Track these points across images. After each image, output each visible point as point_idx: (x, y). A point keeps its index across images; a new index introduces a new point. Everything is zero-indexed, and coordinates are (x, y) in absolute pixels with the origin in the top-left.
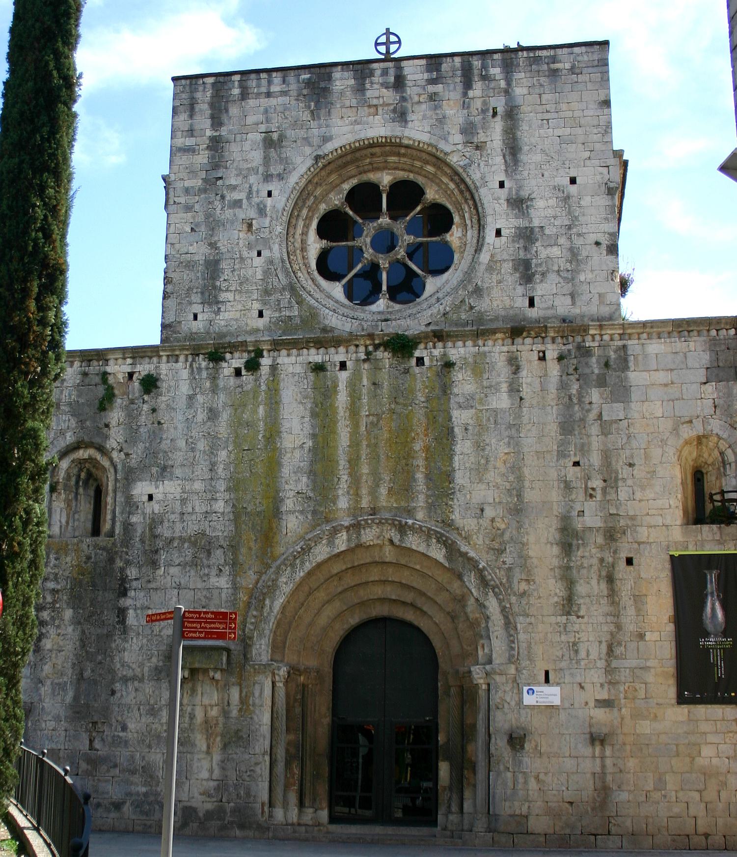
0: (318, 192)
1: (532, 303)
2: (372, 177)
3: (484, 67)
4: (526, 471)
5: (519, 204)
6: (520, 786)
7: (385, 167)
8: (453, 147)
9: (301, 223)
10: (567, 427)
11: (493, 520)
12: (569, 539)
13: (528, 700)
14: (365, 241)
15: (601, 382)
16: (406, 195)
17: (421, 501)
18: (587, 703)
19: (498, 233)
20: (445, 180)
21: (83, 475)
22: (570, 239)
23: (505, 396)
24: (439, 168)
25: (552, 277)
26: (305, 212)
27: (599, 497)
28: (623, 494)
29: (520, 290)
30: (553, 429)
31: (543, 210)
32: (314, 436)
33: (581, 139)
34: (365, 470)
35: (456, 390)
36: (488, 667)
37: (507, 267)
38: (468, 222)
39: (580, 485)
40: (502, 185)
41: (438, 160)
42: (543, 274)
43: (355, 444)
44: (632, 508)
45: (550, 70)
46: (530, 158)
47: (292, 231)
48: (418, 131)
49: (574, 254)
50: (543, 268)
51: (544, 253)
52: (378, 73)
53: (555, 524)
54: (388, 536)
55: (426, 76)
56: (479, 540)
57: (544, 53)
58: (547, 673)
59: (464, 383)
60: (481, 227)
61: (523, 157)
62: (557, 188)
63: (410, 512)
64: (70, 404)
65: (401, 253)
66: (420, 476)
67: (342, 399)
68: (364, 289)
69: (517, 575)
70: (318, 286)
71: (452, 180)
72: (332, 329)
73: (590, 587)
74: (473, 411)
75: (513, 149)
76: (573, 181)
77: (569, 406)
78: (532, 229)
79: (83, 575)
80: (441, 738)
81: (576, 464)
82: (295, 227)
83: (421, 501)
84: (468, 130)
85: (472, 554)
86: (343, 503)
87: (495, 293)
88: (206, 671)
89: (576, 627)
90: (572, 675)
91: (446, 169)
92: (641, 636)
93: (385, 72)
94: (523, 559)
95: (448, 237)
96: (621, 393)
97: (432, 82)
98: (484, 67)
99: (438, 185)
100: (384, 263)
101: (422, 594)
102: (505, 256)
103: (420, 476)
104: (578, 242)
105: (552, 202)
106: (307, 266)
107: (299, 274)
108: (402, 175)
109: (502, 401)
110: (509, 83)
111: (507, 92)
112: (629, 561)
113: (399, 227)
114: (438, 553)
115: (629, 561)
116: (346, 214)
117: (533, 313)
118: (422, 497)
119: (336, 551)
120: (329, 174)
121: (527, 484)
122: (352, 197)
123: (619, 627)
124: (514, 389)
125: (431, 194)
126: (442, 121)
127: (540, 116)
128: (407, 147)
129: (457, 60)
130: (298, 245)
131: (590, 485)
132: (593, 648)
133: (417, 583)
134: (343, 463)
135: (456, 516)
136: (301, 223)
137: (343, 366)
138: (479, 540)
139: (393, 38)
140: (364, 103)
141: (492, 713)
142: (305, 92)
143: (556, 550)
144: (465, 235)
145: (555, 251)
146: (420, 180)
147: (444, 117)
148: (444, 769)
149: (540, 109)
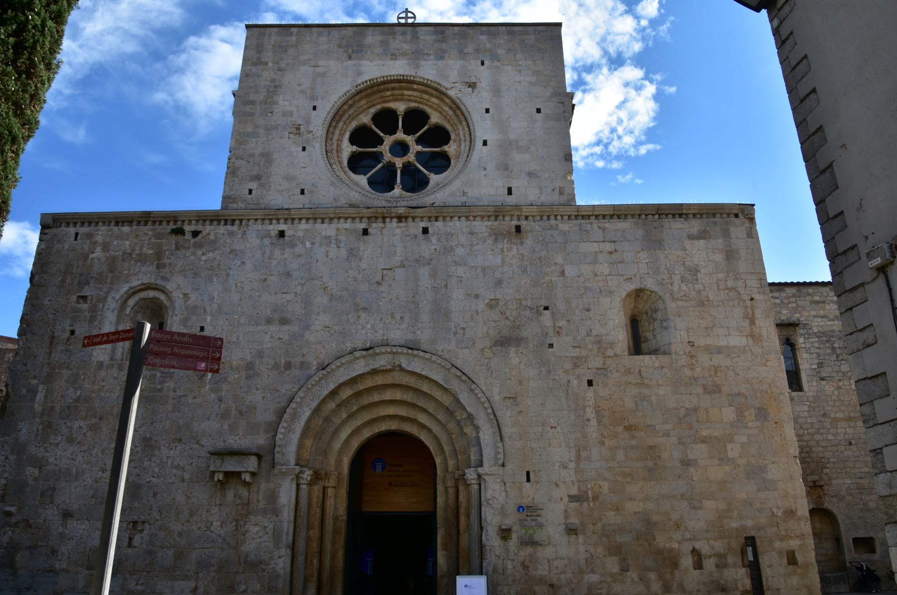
0: (351, 111)
2: (392, 105)
6: (509, 572)
7: (401, 99)
9: (337, 132)
14: (385, 149)
16: (415, 119)
18: (561, 499)
19: (485, 143)
20: (446, 108)
24: (442, 100)
36: (480, 470)
38: (462, 137)
41: (440, 94)
47: (330, 136)
54: (397, 363)
55: (434, 37)
58: (528, 473)
60: (471, 141)
65: (411, 157)
70: (349, 177)
76: (539, 111)
82: (333, 133)
88: (239, 474)
91: (446, 100)
95: (446, 148)
99: (440, 112)
100: (399, 162)
106: (340, 163)
107: (334, 166)
108: (413, 105)
113: (410, 140)
116: (372, 129)
117: (511, 200)
119: (354, 374)
120: (360, 99)
122: (376, 118)
123: (585, 436)
130: (334, 147)
131: (557, 324)
133: (421, 403)
139: (410, 15)
141: (483, 509)
144: (459, 147)
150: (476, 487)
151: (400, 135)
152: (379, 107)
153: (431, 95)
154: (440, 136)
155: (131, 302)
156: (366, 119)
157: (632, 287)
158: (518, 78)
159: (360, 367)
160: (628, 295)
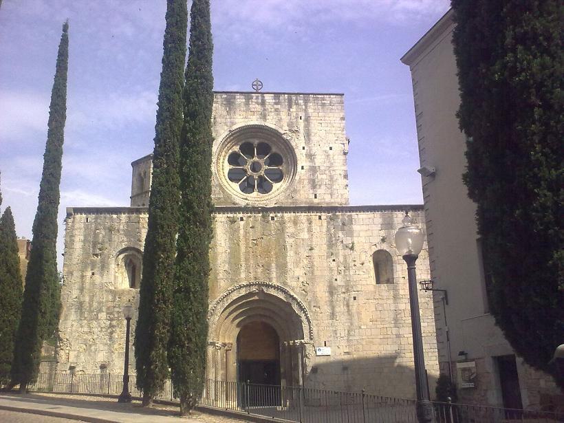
1: (316, 197)
2: (251, 140)
3: (297, 99)
4: (315, 263)
5: (310, 156)
8: (283, 129)
10: (331, 245)
11: (303, 282)
12: (332, 290)
13: (318, 353)
15: (343, 230)
17: (274, 275)
19: (302, 168)
21: (128, 261)
22: (330, 171)
23: (306, 233)
25: (323, 187)
26: (223, 153)
27: (343, 273)
28: (352, 273)
29: (311, 191)
30: (325, 247)
31: (319, 161)
32: (230, 248)
33: (334, 132)
35: (287, 231)
36: (302, 341)
37: (306, 182)
39: (336, 269)
40: (304, 148)
42: (320, 186)
43: (247, 252)
44: (356, 278)
45: (322, 103)
46: (314, 139)
48: (271, 123)
49: (331, 178)
50: (320, 183)
51: (320, 177)
52: (254, 97)
53: (327, 284)
55: (274, 101)
56: (298, 290)
57: (320, 96)
59: (290, 229)
61: (312, 138)
62: (326, 151)
63: (270, 279)
64: (123, 230)
66: (273, 265)
67: (242, 232)
68: (247, 188)
69: (313, 304)
71: (282, 144)
72: (237, 204)
73: (340, 308)
74: (294, 239)
76: (331, 148)
77: (331, 238)
78: (315, 167)
80: (282, 370)
81: (334, 260)
83: (274, 275)
84: (290, 125)
85: (295, 296)
86: (243, 275)
87: (302, 192)
89: (336, 324)
90: (335, 343)
92: (360, 328)
93: (257, 98)
94: (315, 297)
96: (350, 233)
97: (276, 104)
98: (297, 99)
100: (256, 176)
101: (274, 312)
102: (305, 177)
103: (273, 265)
104: (333, 173)
105: (323, 157)
108: (262, 140)
109: (305, 235)
110: (306, 107)
111: (306, 111)
112: (355, 298)
113: (262, 161)
114: (281, 296)
115: (355, 298)
117: (316, 201)
118: (275, 273)
121: (315, 268)
123: (352, 324)
124: (310, 230)
125: (274, 150)
126: (280, 120)
127: (318, 121)
128: (266, 129)
129: (286, 96)
130: (221, 167)
131: (339, 269)
132: (342, 331)
134: (242, 259)
135: (288, 281)
136: (222, 158)
137: (242, 219)
138: (298, 290)
140: (248, 110)
142: (224, 103)
143: (327, 294)
145: (324, 176)
146: (270, 144)
147: (281, 118)
148: (283, 383)
149: (319, 118)
150: (301, 349)
151: (256, 159)
152: (244, 141)
154: (275, 160)
155: (121, 256)
156: (236, 149)
157: (375, 249)
158: (320, 128)
159: (243, 292)
160: (375, 253)
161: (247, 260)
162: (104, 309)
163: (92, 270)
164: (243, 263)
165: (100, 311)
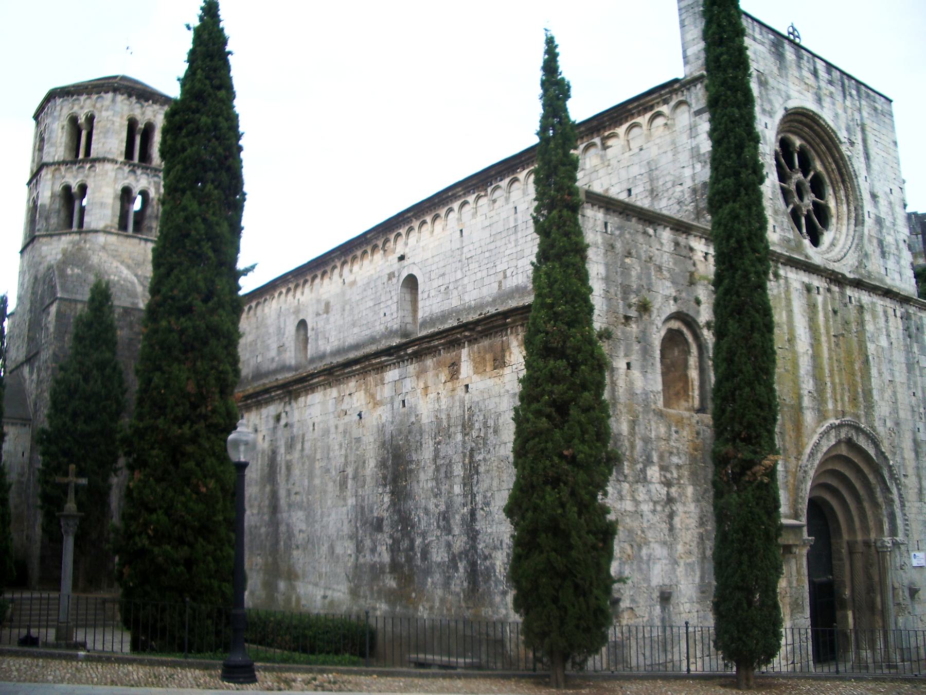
34: (837, 381)
43: (830, 358)
48: (827, 115)
75: (867, 157)
79: (696, 451)
135: (876, 424)
153: (823, 142)
161: (832, 376)
162: (655, 459)
163: (626, 355)
164: (828, 380)
165: (648, 462)
